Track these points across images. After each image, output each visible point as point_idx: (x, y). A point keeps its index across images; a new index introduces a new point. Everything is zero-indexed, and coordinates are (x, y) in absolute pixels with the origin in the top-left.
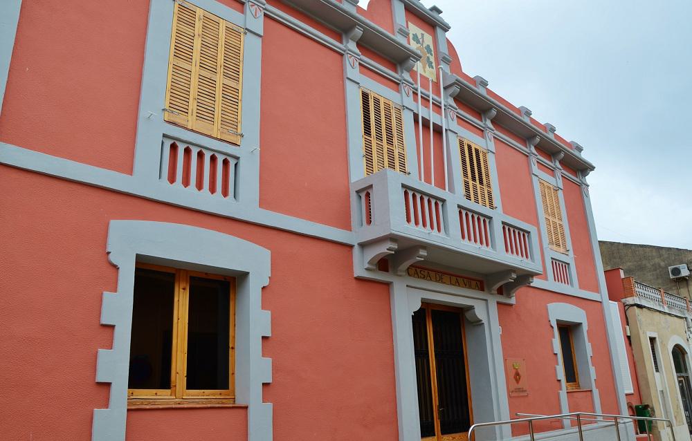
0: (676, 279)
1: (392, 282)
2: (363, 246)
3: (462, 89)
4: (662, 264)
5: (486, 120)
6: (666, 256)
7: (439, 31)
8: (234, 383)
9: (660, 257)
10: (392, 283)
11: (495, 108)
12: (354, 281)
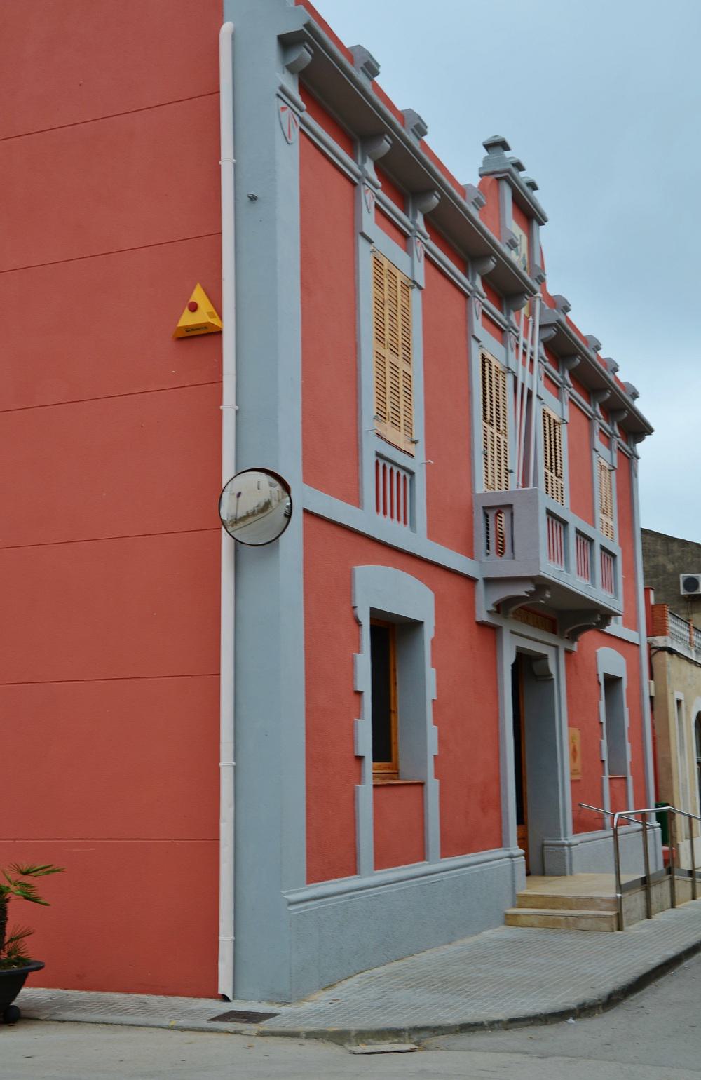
0: (689, 596)
1: (501, 627)
2: (489, 581)
3: (559, 332)
4: (670, 567)
5: (364, 161)
6: (679, 554)
7: (535, 224)
8: (397, 754)
9: (668, 554)
10: (500, 628)
11: (496, 257)
12: (475, 626)
